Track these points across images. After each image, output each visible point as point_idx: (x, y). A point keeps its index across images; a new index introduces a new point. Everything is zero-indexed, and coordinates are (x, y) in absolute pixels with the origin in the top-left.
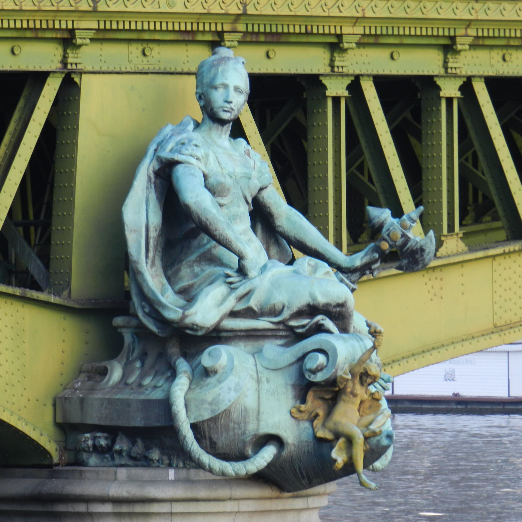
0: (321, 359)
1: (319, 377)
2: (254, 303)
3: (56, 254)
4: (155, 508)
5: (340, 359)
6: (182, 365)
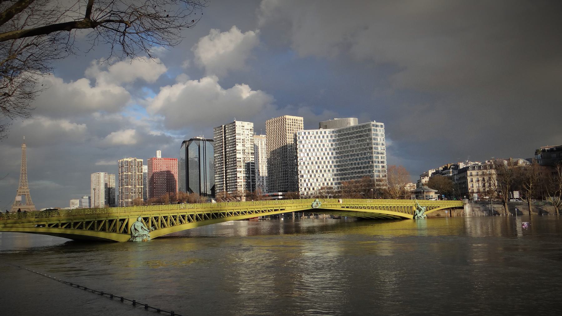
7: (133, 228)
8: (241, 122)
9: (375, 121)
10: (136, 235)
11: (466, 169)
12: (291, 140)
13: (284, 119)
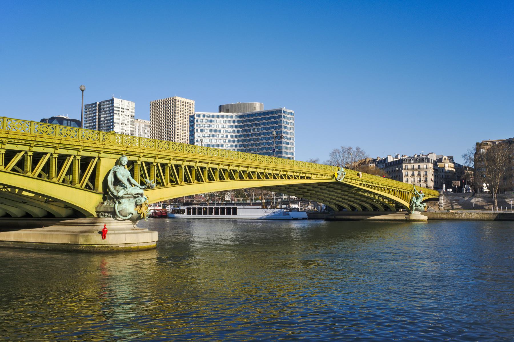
0: (139, 201)
1: (139, 204)
2: (128, 193)
3: (96, 185)
4: (112, 224)
5: (142, 201)
6: (117, 202)
7: (111, 179)
8: (121, 100)
9: (285, 108)
10: (121, 194)
11: (401, 162)
12: (181, 125)
13: (174, 101)
